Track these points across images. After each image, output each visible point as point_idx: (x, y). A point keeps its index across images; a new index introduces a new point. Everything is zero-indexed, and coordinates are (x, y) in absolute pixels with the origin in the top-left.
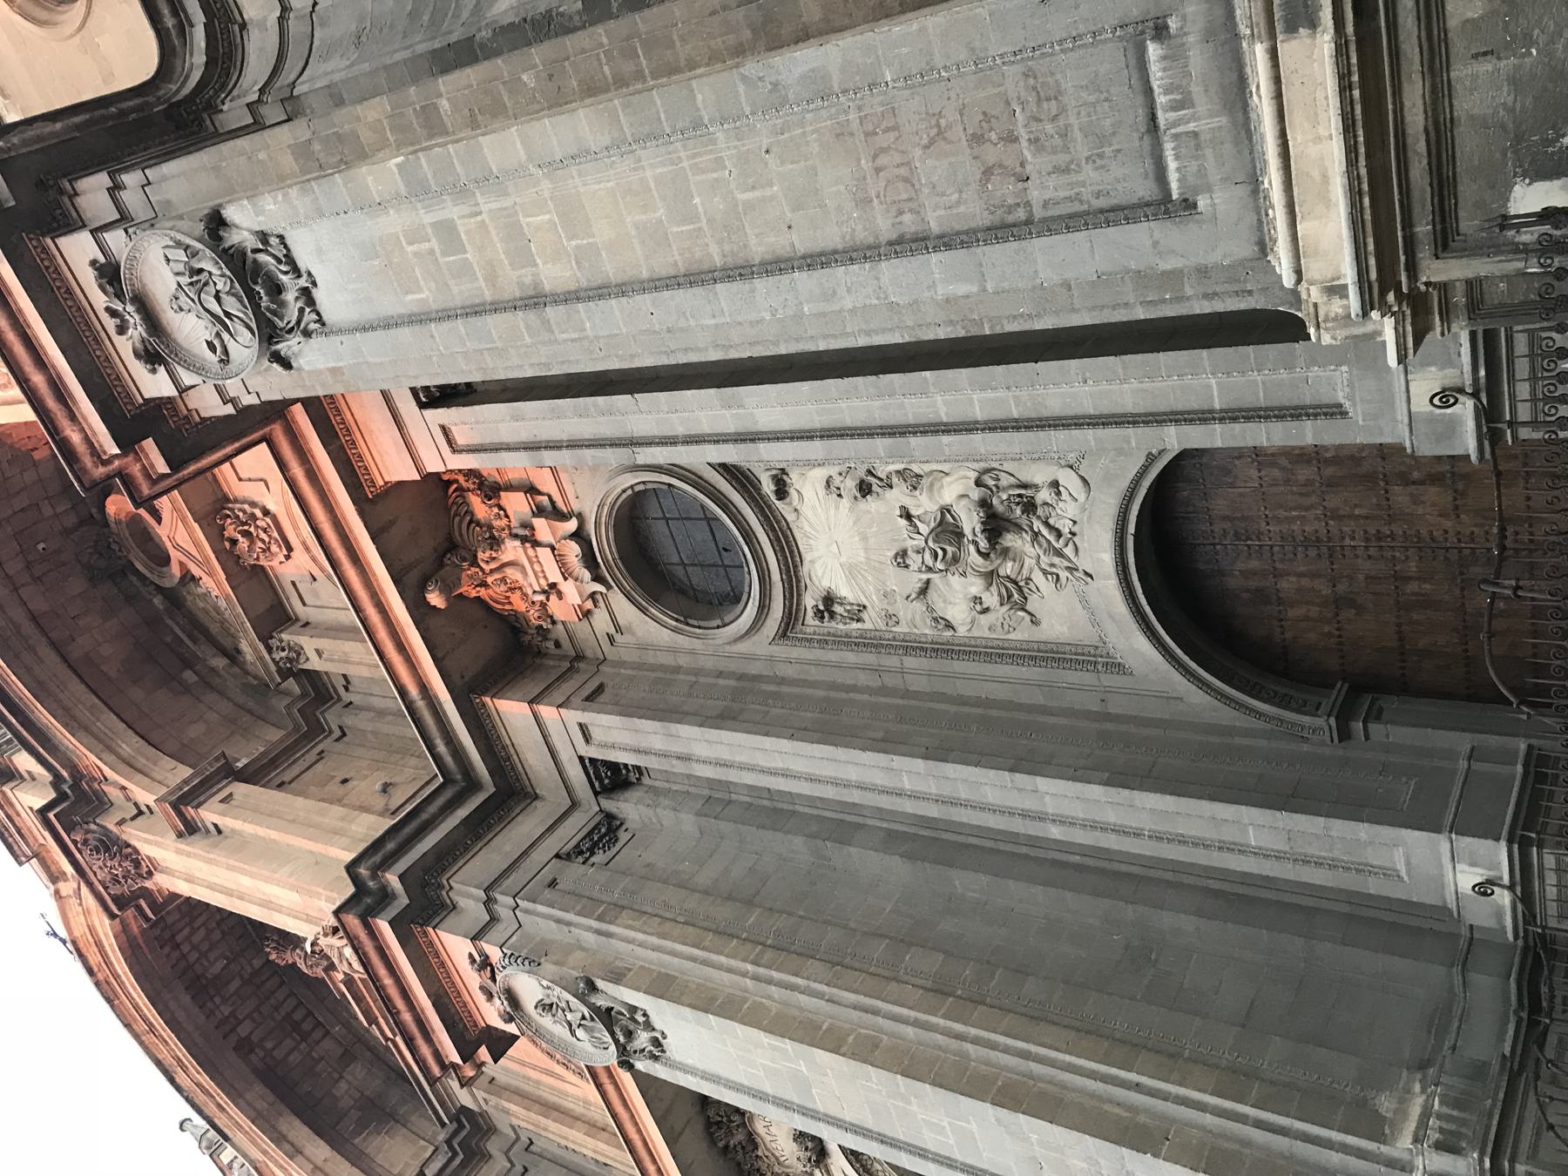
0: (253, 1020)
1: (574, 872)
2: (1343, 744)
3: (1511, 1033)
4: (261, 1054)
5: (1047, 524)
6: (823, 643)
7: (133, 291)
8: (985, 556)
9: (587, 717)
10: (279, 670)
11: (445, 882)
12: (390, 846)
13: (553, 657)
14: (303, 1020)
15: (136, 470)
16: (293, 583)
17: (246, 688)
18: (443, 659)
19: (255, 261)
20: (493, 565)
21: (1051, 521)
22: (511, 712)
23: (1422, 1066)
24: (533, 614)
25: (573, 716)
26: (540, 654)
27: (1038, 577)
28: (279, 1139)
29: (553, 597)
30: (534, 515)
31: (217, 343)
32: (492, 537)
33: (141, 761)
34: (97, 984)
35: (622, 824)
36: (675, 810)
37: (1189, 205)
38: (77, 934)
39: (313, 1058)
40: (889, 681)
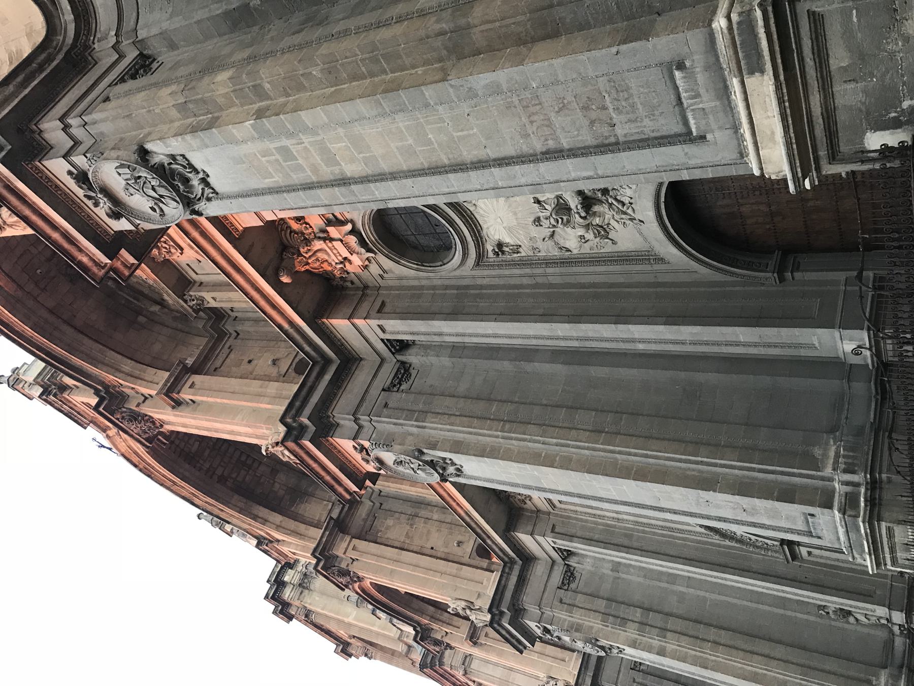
0: (222, 466)
1: (395, 398)
2: (782, 284)
3: (873, 407)
4: (232, 481)
5: (616, 199)
6: (500, 266)
7: (99, 187)
8: (584, 218)
9: (381, 322)
10: (194, 310)
12: (298, 404)
13: (351, 289)
14: (246, 460)
15: (118, 264)
16: (188, 265)
17: (175, 319)
18: (297, 307)
19: (170, 168)
20: (310, 254)
21: (618, 198)
22: (340, 325)
23: (832, 430)
24: (337, 273)
25: (374, 323)
26: (343, 288)
27: (613, 222)
28: (255, 518)
29: (347, 264)
30: (327, 225)
31: (155, 207)
32: (305, 239)
33: (137, 373)
34: (141, 470)
35: (410, 365)
36: (438, 356)
37: (703, 138)
38: (123, 451)
40: (540, 280)
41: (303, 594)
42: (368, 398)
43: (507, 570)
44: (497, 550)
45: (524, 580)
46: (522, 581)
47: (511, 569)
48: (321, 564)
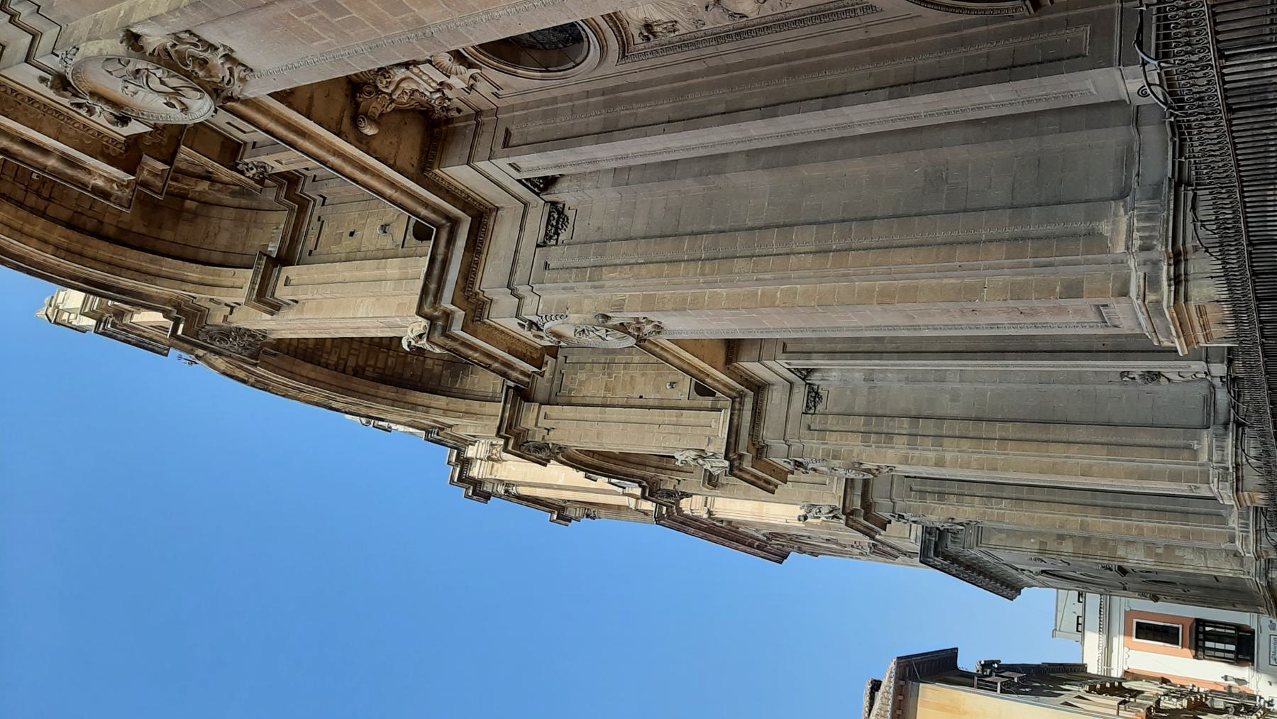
0: (354, 355)
1: (555, 254)
3: (1170, 153)
4: (371, 369)
6: (654, 53)
9: (512, 160)
10: (257, 182)
11: (479, 291)
12: (433, 286)
13: (459, 120)
16: (229, 123)
17: (233, 194)
18: (395, 162)
20: (392, 88)
22: (458, 173)
23: (1122, 194)
25: (503, 163)
26: (449, 121)
28: (414, 406)
33: (209, 279)
34: (252, 386)
35: (564, 205)
36: (597, 188)
39: (402, 356)
40: (713, 63)
41: (495, 468)
42: (521, 258)
43: (737, 406)
44: (720, 387)
45: (759, 413)
46: (757, 413)
47: (742, 403)
48: (511, 443)
